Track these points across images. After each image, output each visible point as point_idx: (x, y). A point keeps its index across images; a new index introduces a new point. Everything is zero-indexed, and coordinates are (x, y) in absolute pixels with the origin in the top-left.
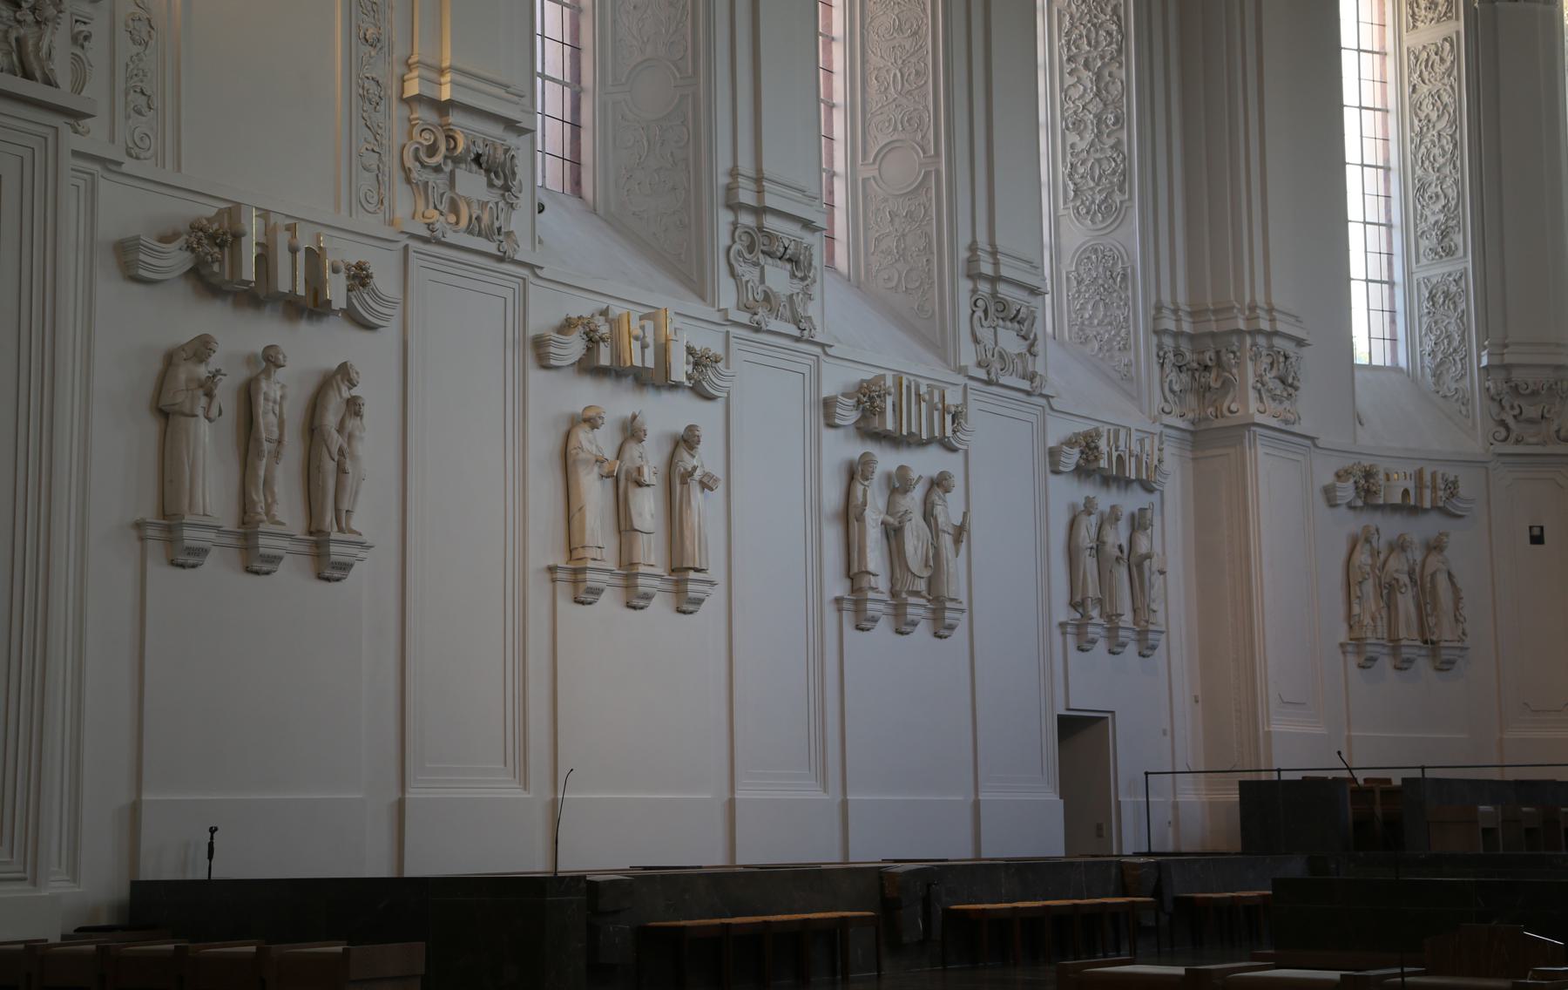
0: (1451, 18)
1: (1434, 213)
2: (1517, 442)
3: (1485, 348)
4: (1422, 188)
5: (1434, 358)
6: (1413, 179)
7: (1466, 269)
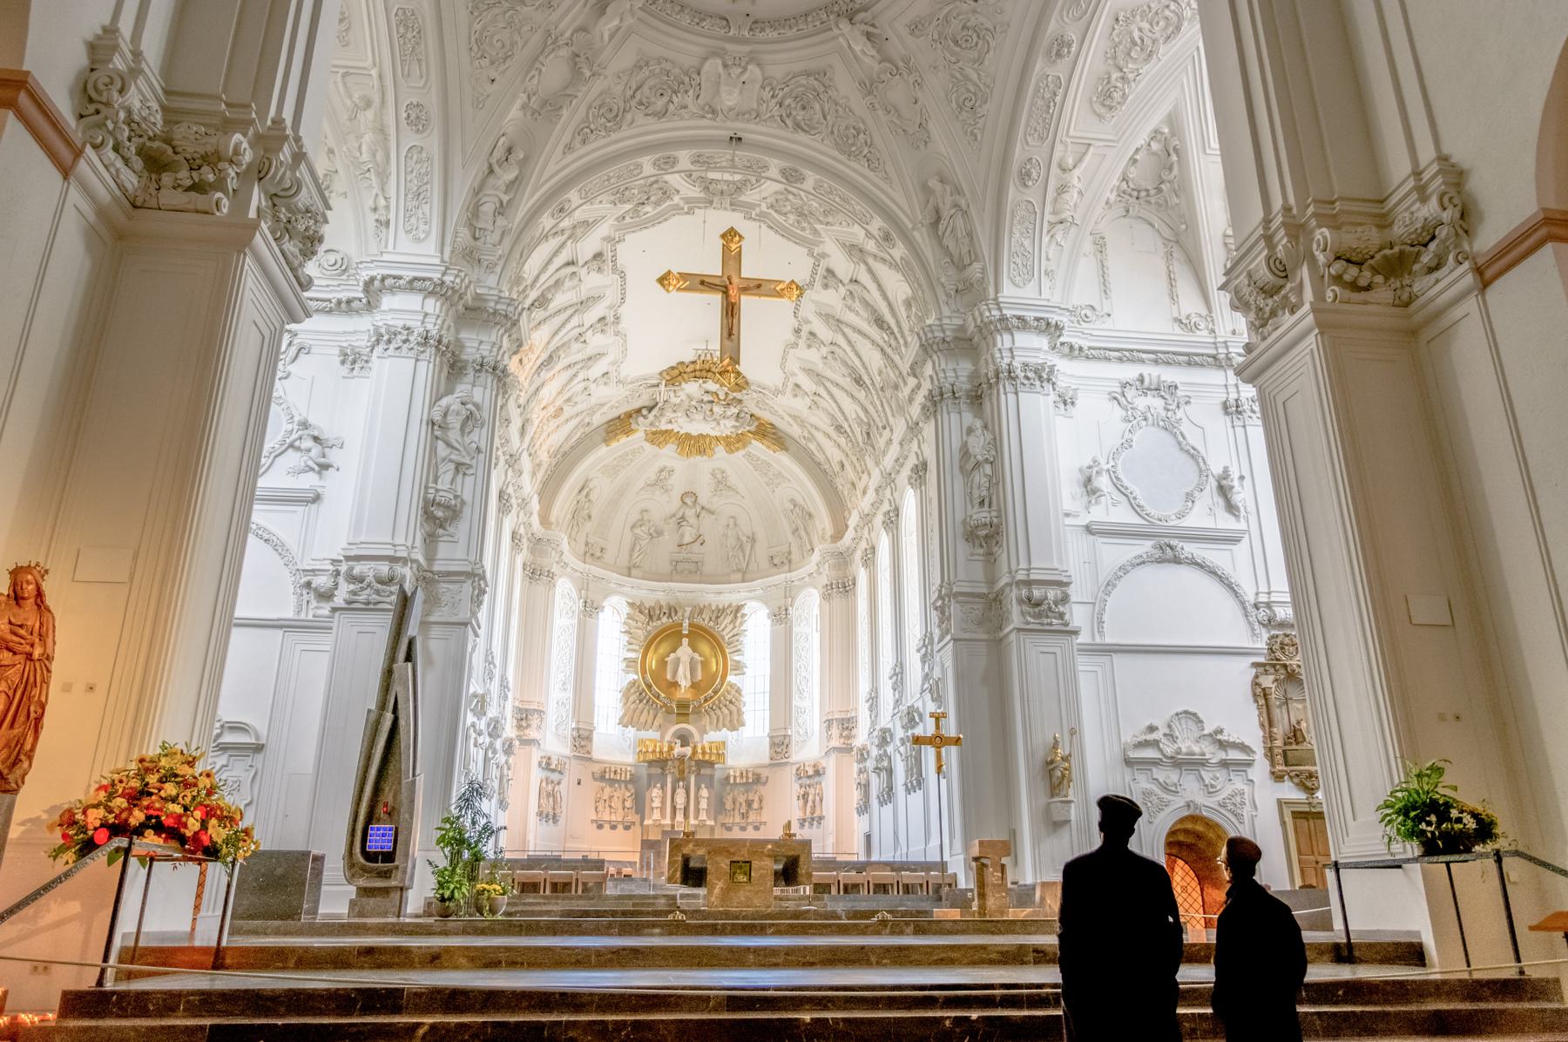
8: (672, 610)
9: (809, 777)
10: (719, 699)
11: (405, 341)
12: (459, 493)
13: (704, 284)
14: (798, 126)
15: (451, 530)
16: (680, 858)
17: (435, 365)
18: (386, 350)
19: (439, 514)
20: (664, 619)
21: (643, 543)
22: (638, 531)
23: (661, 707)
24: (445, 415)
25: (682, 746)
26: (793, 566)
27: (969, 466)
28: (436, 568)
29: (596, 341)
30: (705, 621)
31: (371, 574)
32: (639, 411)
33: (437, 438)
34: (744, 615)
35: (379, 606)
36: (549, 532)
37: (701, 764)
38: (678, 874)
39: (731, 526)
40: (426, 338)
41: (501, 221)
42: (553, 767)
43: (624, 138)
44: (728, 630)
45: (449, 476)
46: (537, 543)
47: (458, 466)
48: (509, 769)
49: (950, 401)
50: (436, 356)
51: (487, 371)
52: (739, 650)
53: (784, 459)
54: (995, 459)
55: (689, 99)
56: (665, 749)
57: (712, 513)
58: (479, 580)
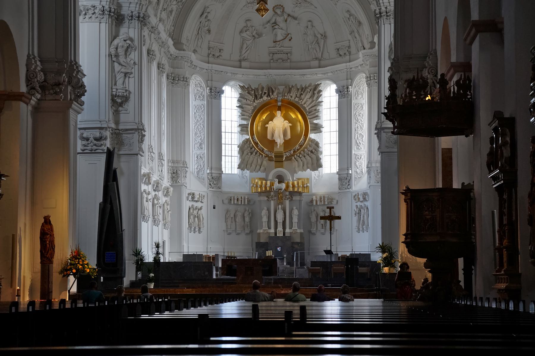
0: (203, 101)
1: (199, 140)
2: (212, 188)
3: (208, 169)
4: (196, 134)
5: (197, 169)
6: (194, 132)
7: (205, 152)
8: (270, 90)
9: (361, 202)
10: (304, 151)
11: (93, 14)
12: (127, 89)
15: (125, 106)
16: (226, 266)
17: (109, 24)
18: (84, 18)
19: (119, 101)
20: (265, 98)
21: (248, 43)
22: (244, 35)
23: (265, 157)
24: (117, 48)
25: (280, 182)
26: (352, 57)
28: (121, 127)
30: (292, 97)
31: (92, 136)
33: (114, 61)
34: (320, 91)
35: (97, 151)
36: (182, 52)
37: (292, 194)
38: (225, 272)
39: (310, 27)
40: (104, 10)
42: (196, 199)
44: (308, 103)
45: (122, 80)
46: (173, 59)
47: (126, 74)
48: (168, 205)
49: (385, 17)
50: (109, 18)
51: (135, 19)
52: (317, 116)
57: (295, 18)
58: (141, 131)
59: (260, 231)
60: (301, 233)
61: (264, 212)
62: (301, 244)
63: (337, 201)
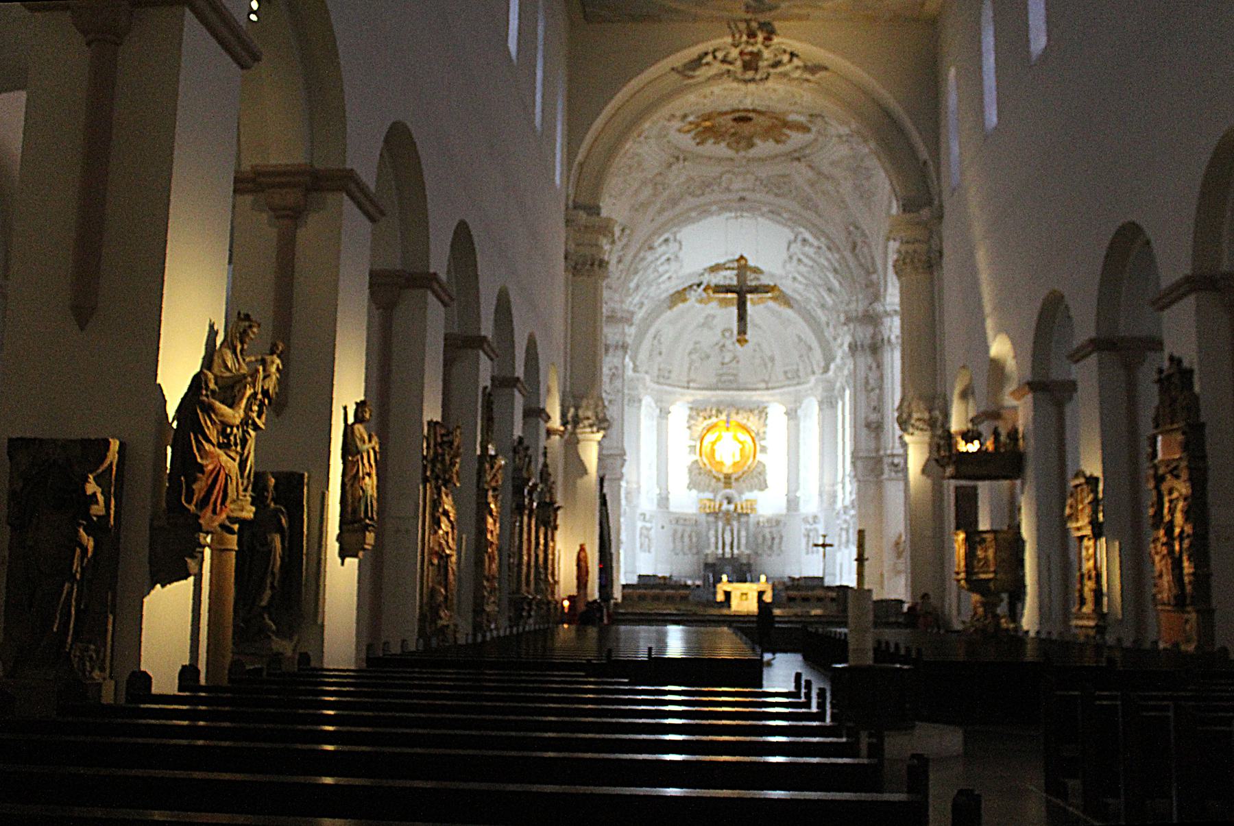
13: (728, 289)
14: (776, 195)
22: (694, 357)
25: (729, 503)
27: (869, 388)
29: (661, 269)
32: (691, 287)
37: (740, 515)
41: (621, 266)
43: (682, 206)
53: (788, 312)
54: (881, 388)
55: (715, 187)
56: (717, 506)
59: (708, 551)
60: (749, 556)
61: (712, 533)
62: (749, 565)
63: (785, 524)
